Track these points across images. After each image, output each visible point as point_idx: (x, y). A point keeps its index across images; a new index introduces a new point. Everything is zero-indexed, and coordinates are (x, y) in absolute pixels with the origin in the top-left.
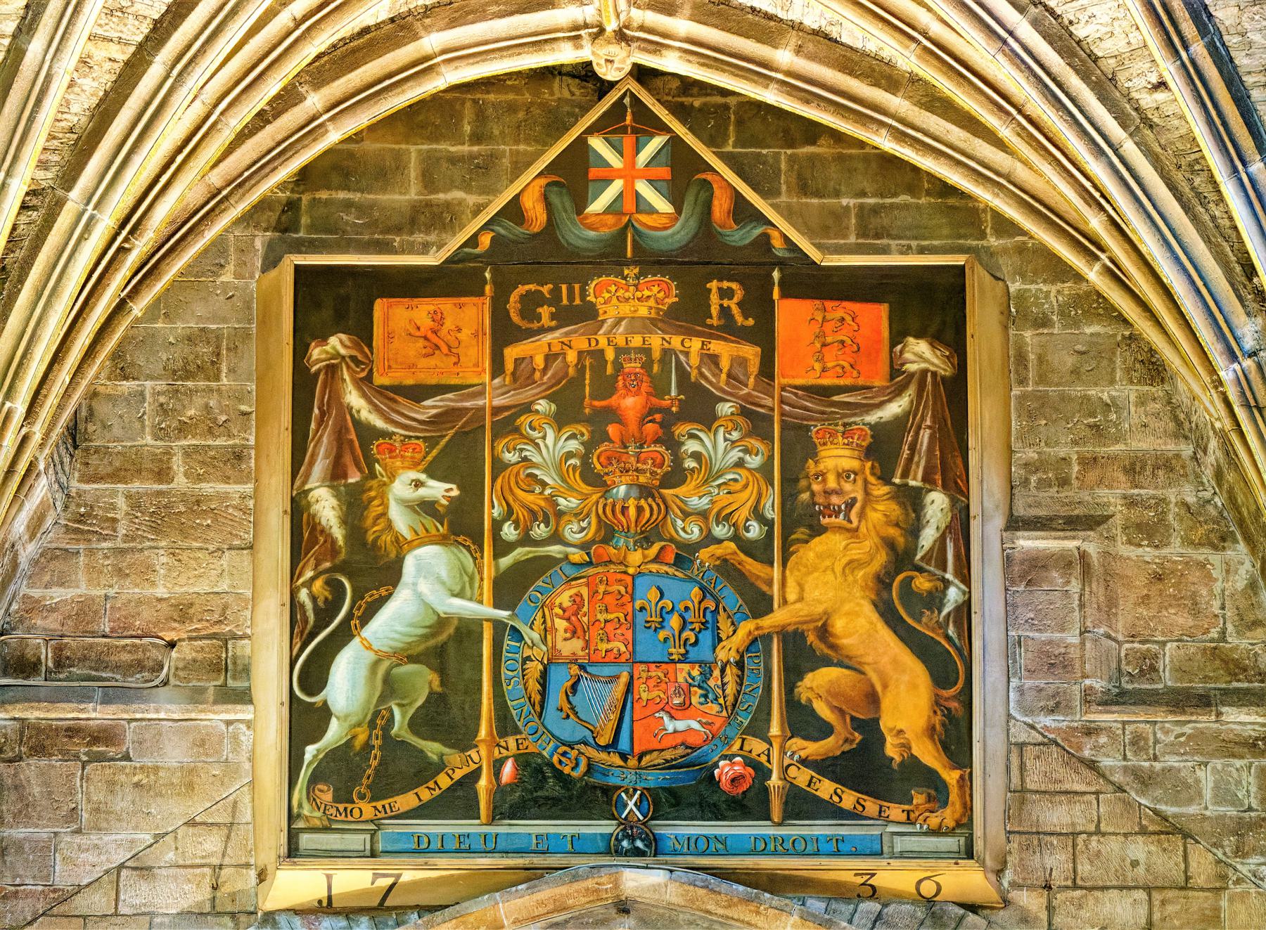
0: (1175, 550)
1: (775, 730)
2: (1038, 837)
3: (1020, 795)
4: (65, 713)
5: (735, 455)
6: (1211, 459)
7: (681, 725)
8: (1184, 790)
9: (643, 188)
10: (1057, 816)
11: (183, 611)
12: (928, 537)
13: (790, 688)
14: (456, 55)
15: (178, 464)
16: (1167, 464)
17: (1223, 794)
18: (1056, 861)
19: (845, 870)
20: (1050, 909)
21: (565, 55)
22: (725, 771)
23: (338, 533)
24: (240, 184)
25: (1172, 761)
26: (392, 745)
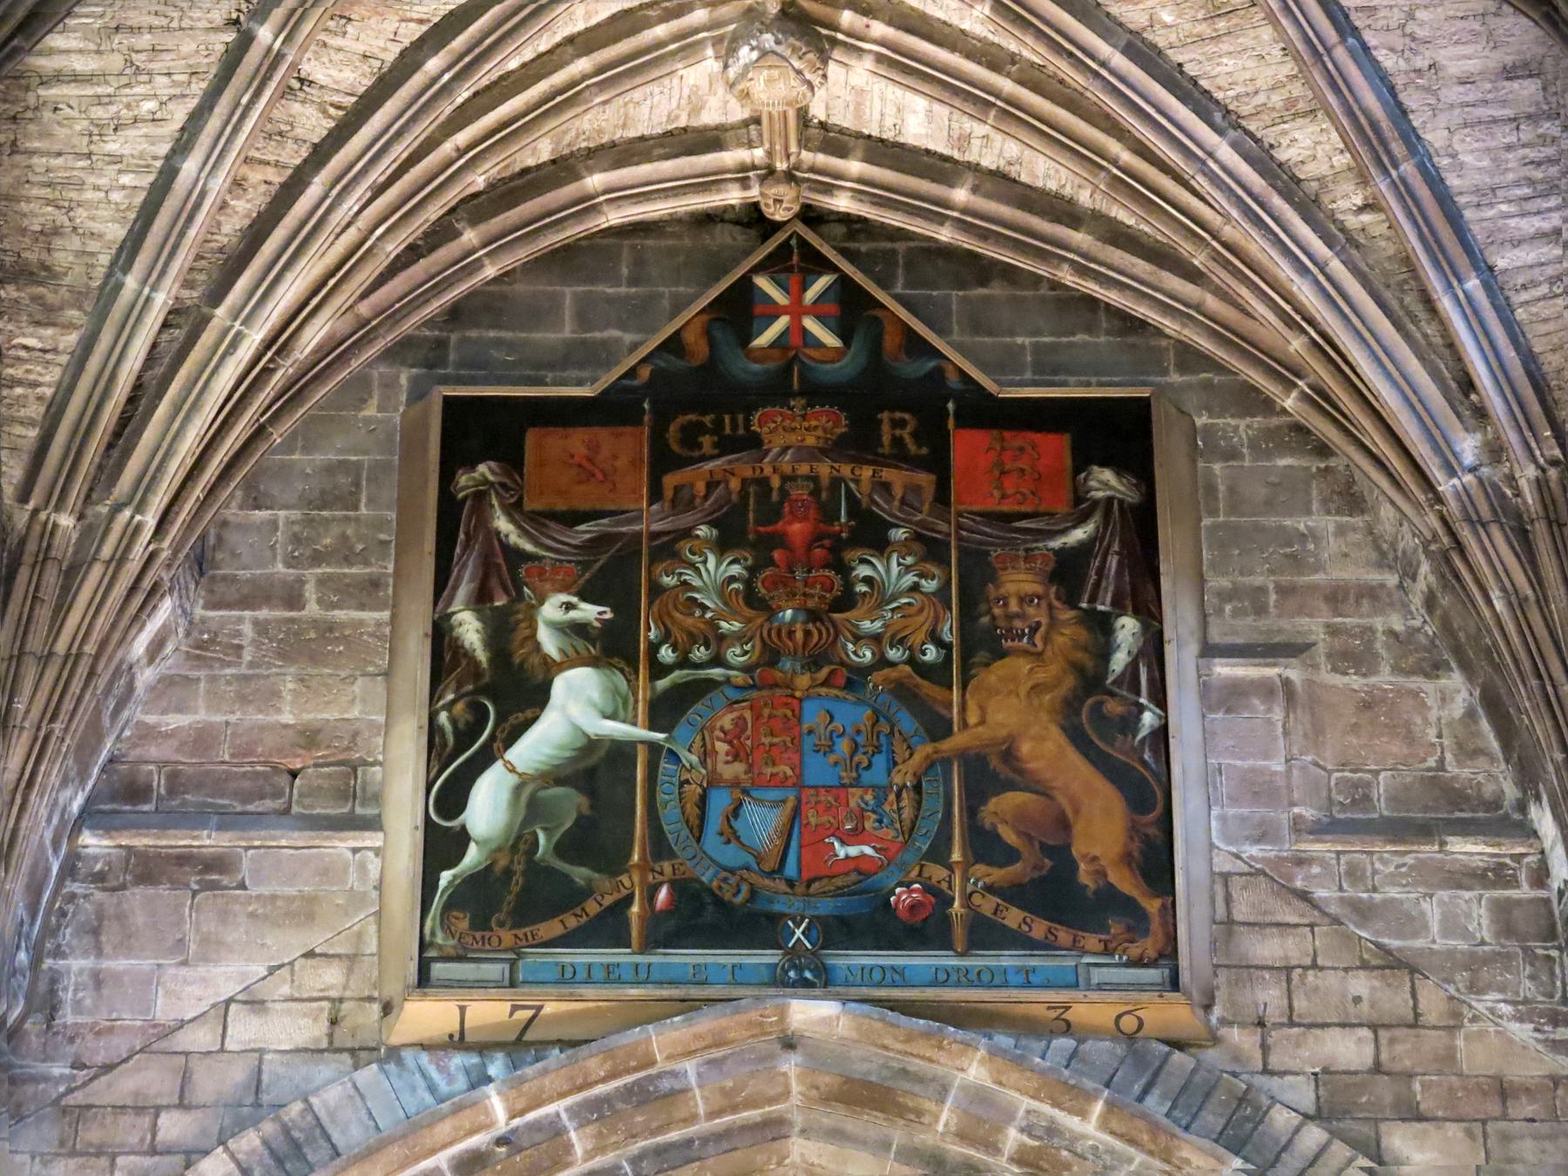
0: (1384, 678)
1: (956, 856)
2: (1248, 970)
3: (1228, 926)
4: (179, 840)
5: (910, 579)
6: (1421, 585)
7: (853, 851)
8: (1412, 923)
9: (810, 323)
10: (1267, 949)
11: (310, 737)
12: (1119, 661)
13: (971, 811)
14: (620, 195)
15: (310, 592)
16: (1371, 593)
17: (1452, 926)
18: (1270, 996)
19: (1037, 1002)
20: (1265, 1048)
21: (733, 196)
22: (902, 897)
23: (482, 656)
24: (391, 315)
25: (1393, 893)
26: (535, 870)
